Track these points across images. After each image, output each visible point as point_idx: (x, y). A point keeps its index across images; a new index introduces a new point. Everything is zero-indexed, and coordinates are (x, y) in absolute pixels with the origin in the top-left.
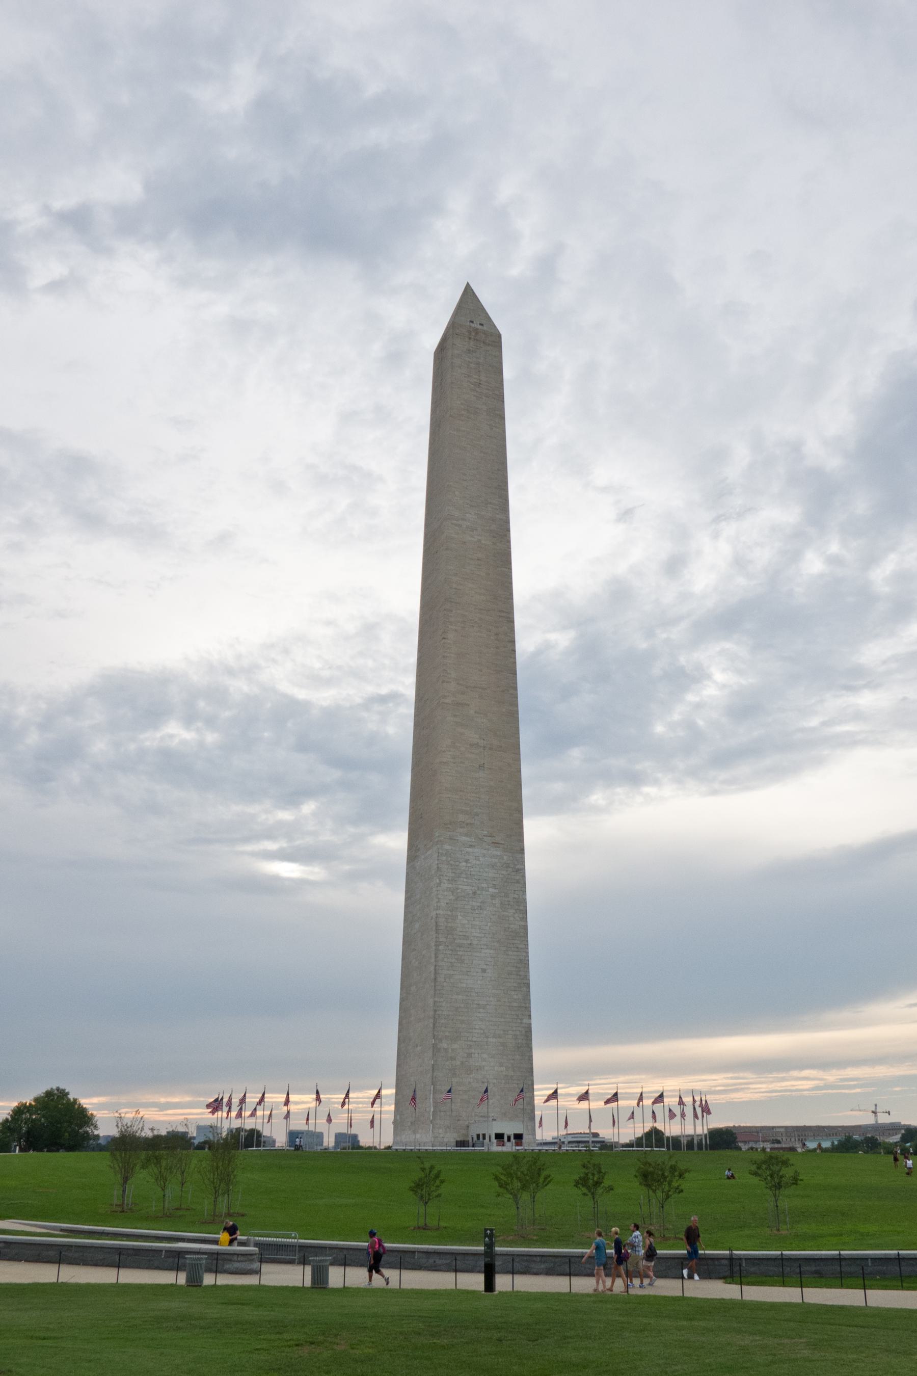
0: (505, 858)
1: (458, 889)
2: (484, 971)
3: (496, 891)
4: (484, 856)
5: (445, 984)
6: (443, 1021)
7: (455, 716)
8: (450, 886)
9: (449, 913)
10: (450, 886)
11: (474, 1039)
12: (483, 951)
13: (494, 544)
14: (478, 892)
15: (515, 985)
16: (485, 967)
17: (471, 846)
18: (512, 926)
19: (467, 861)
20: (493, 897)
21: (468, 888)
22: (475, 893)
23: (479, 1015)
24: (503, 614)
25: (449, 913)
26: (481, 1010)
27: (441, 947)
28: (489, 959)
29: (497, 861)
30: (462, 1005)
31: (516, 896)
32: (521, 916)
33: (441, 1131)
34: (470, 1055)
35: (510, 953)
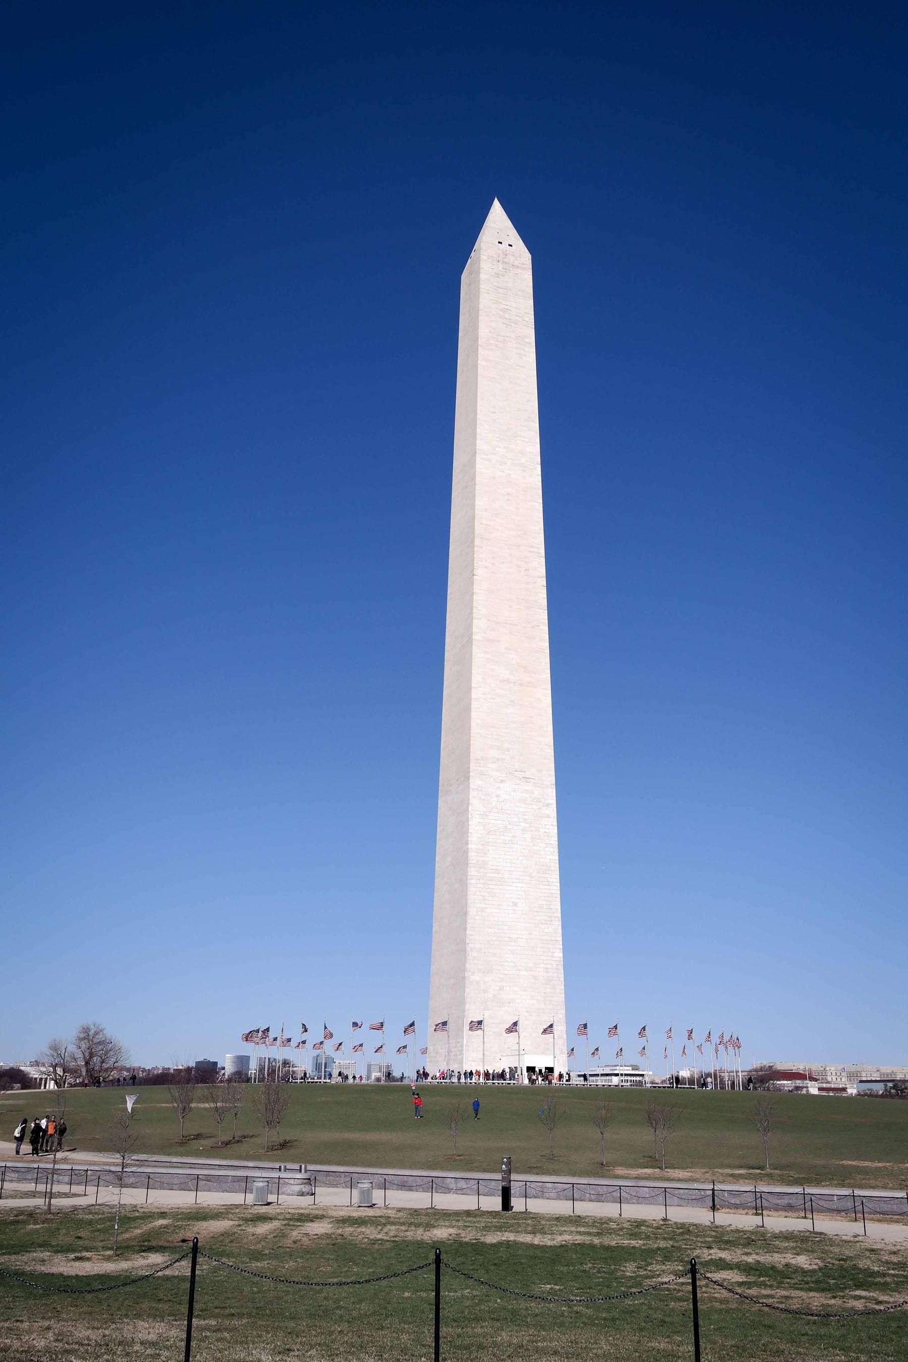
0: (536, 792)
1: (489, 823)
2: (515, 904)
4: (515, 791)
5: (477, 917)
6: (475, 954)
7: (486, 652)
8: (481, 820)
9: (481, 847)
10: (481, 820)
11: (506, 972)
13: (524, 478)
14: (509, 827)
15: (545, 918)
16: (516, 901)
17: (502, 781)
21: (499, 822)
23: (510, 948)
24: (532, 549)
25: (481, 847)
27: (473, 881)
28: (520, 893)
29: (526, 795)
30: (494, 938)
33: (473, 1063)
34: (501, 988)
35: (541, 887)
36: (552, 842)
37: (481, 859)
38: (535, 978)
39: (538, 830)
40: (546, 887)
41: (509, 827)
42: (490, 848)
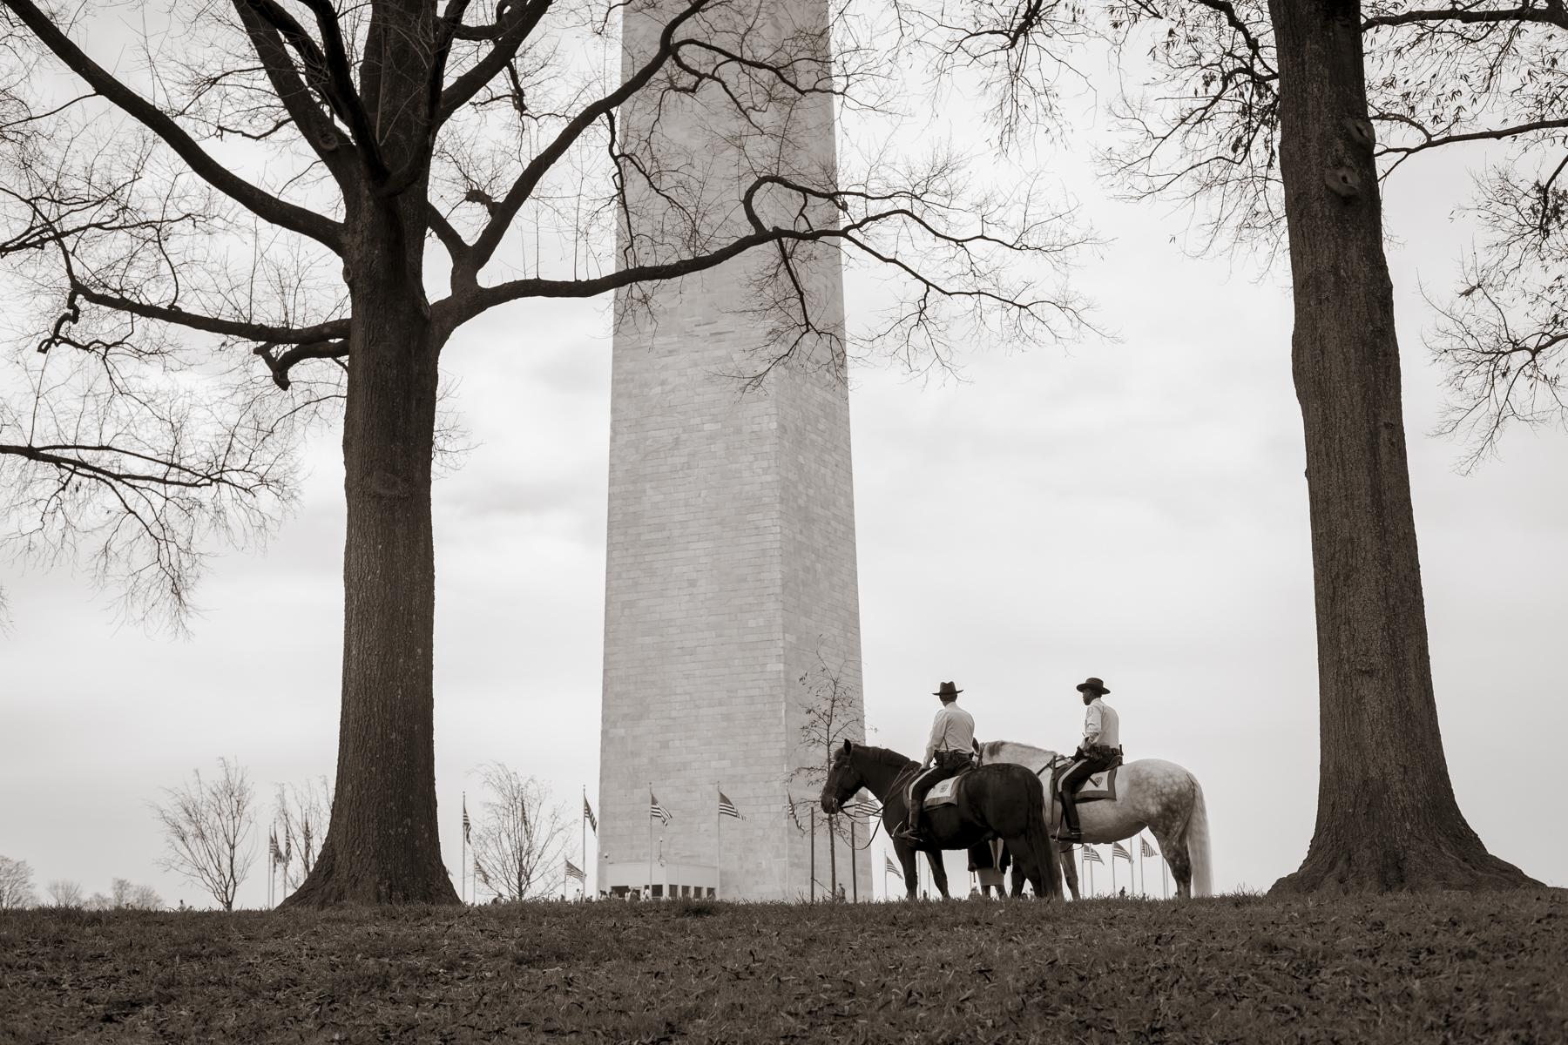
1: (646, 439)
3: (719, 426)
8: (633, 436)
9: (631, 488)
10: (633, 436)
11: (674, 714)
12: (693, 546)
14: (684, 436)
18: (747, 488)
19: (663, 383)
20: (712, 438)
22: (677, 441)
25: (631, 488)
26: (687, 658)
27: (615, 554)
31: (756, 428)
32: (765, 464)
34: (665, 745)
36: (767, 448)
37: (631, 509)
38: (727, 718)
39: (738, 431)
40: (753, 539)
41: (684, 436)
42: (648, 486)
